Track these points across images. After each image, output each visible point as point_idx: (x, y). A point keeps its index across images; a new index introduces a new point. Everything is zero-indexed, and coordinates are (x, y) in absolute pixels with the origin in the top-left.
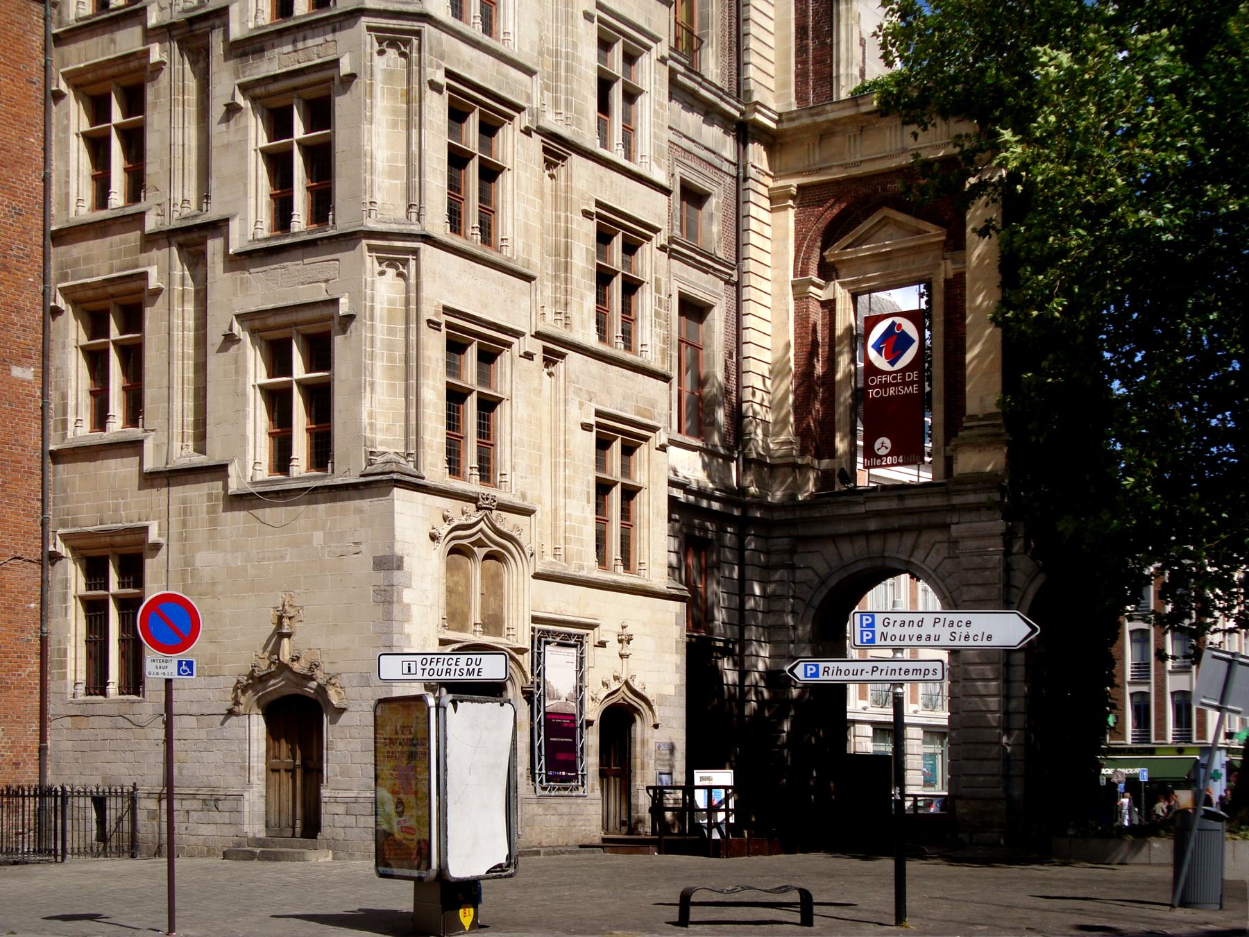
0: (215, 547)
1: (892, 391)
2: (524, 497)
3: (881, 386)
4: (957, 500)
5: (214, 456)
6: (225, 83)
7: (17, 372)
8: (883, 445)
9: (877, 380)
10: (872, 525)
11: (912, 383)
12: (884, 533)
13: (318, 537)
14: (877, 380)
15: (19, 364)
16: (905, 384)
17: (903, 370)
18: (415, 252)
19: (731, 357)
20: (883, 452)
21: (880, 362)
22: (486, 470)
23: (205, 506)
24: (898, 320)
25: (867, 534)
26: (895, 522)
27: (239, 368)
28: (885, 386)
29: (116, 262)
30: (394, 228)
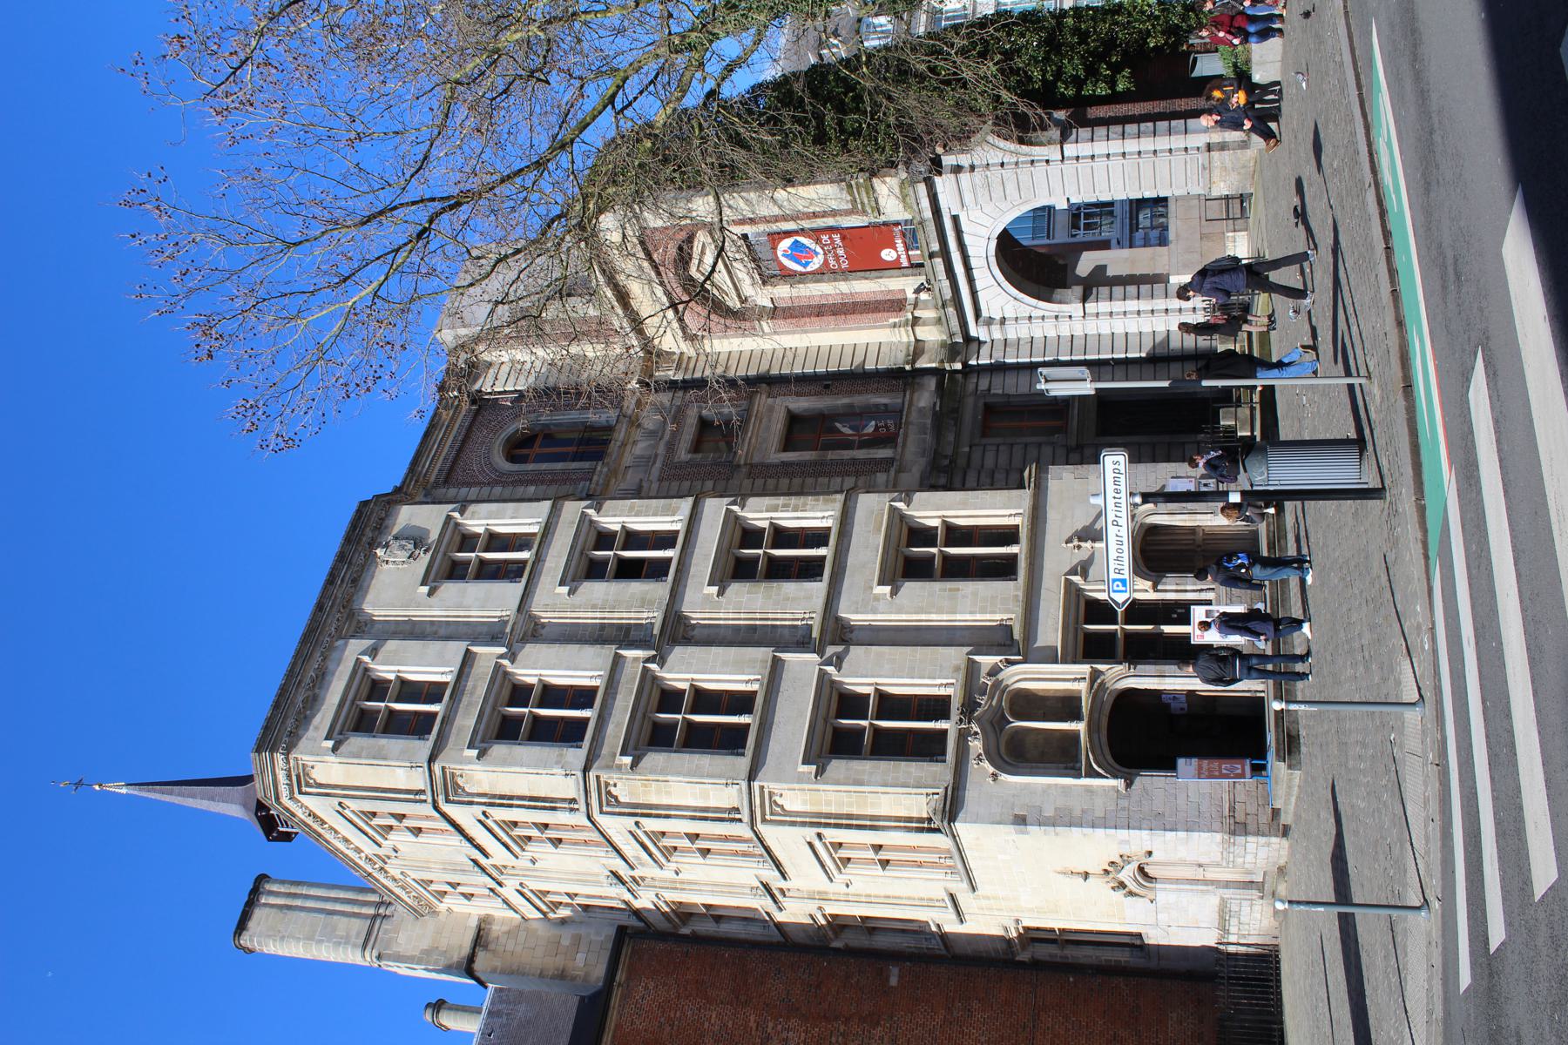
1: (841, 252)
2: (957, 669)
4: (928, 214)
7: (894, 981)
9: (832, 262)
14: (832, 262)
15: (887, 979)
19: (827, 387)
22: (936, 707)
24: (780, 253)
28: (837, 258)
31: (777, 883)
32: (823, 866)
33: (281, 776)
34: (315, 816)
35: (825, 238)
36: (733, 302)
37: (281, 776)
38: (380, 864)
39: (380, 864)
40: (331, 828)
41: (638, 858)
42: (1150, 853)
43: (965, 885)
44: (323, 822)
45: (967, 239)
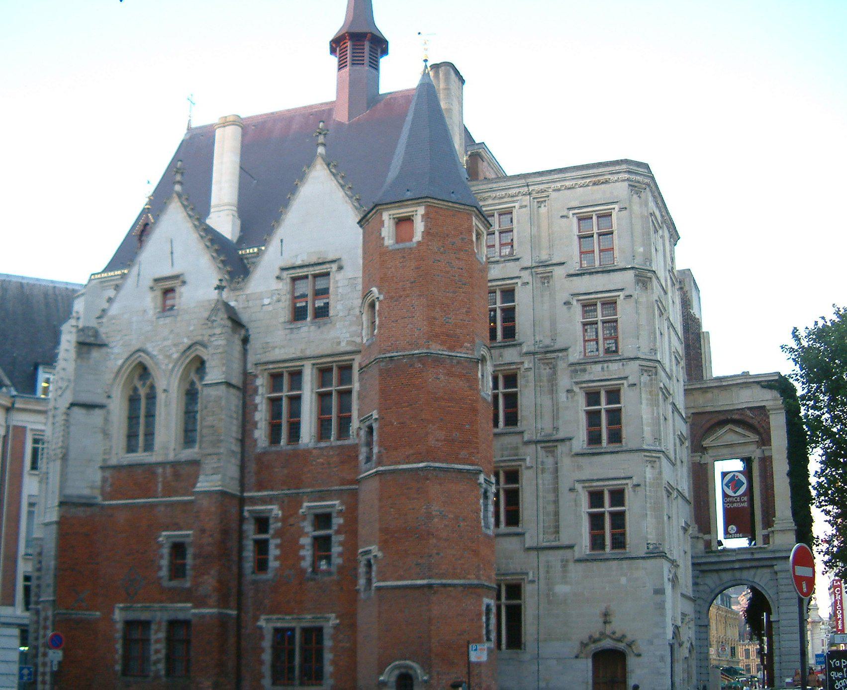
0: (566, 583)
1: (735, 505)
3: (730, 502)
5: (565, 540)
6: (564, 381)
8: (733, 528)
10: (737, 565)
11: (744, 502)
12: (741, 569)
13: (623, 580)
16: (741, 502)
17: (740, 496)
18: (659, 458)
20: (732, 532)
21: (730, 492)
23: (559, 564)
25: (733, 569)
26: (748, 564)
27: (577, 504)
28: (733, 502)
29: (505, 453)
30: (652, 448)
31: (561, 448)
32: (598, 480)
33: (638, 178)
34: (603, 183)
35: (745, 498)
36: (705, 443)
37: (638, 178)
38: (534, 195)
39: (534, 195)
40: (588, 186)
41: (584, 370)
42: (639, 655)
43: (577, 555)
44: (595, 184)
45: (752, 572)
